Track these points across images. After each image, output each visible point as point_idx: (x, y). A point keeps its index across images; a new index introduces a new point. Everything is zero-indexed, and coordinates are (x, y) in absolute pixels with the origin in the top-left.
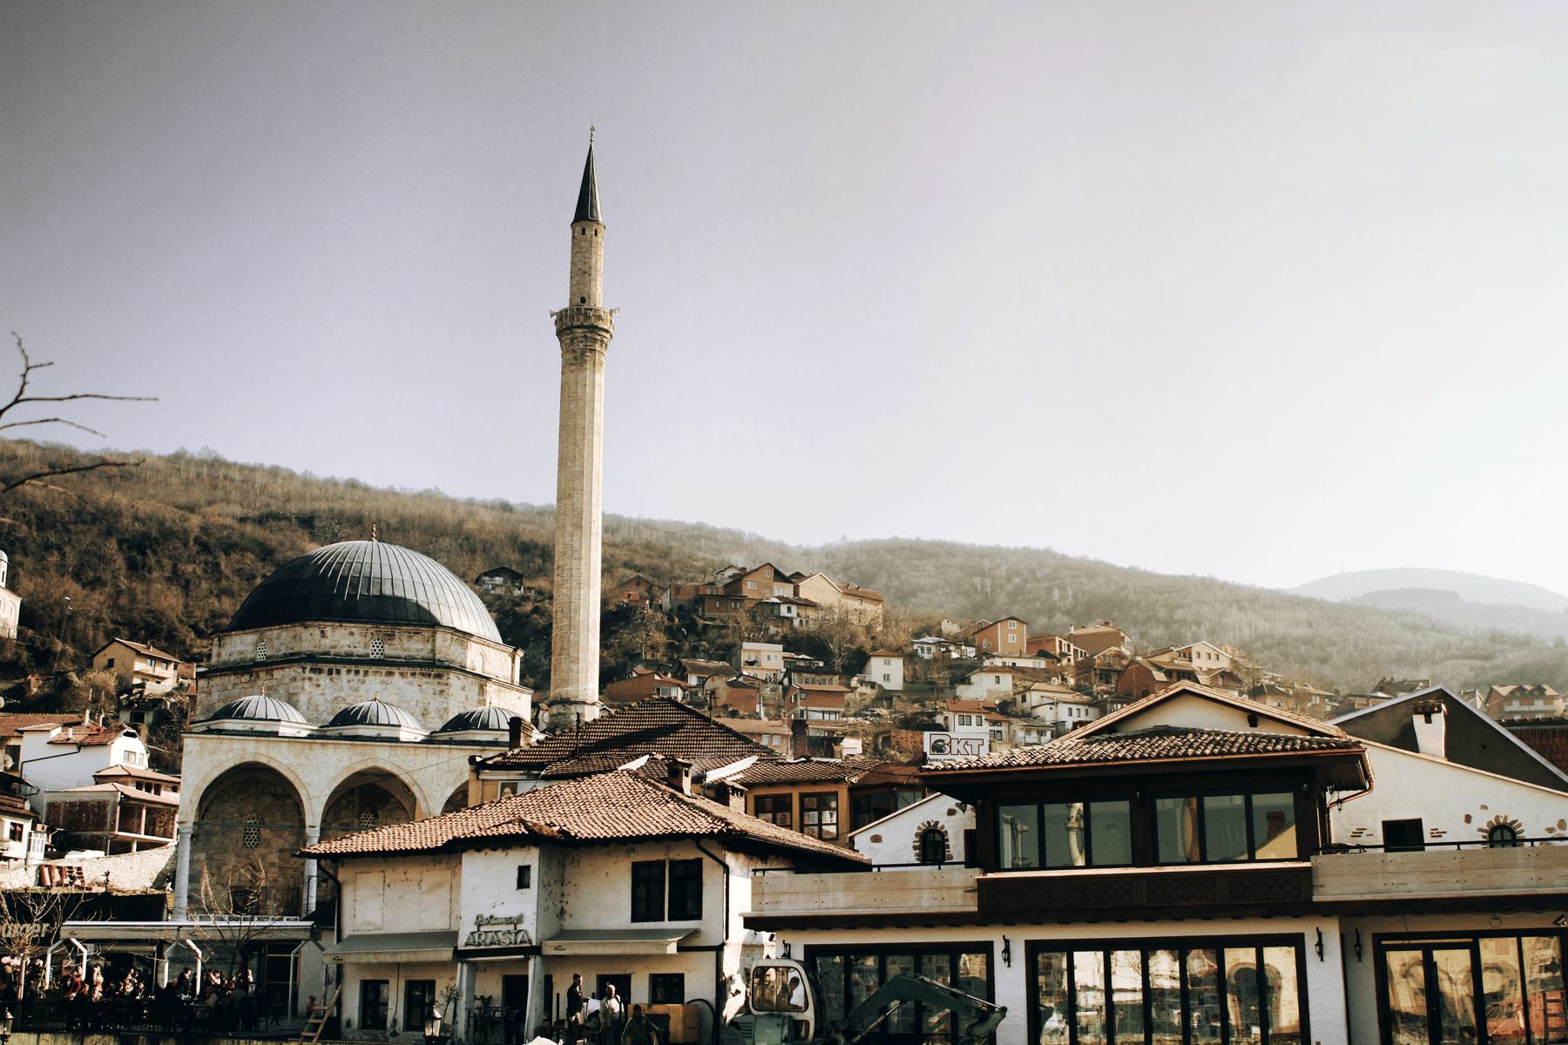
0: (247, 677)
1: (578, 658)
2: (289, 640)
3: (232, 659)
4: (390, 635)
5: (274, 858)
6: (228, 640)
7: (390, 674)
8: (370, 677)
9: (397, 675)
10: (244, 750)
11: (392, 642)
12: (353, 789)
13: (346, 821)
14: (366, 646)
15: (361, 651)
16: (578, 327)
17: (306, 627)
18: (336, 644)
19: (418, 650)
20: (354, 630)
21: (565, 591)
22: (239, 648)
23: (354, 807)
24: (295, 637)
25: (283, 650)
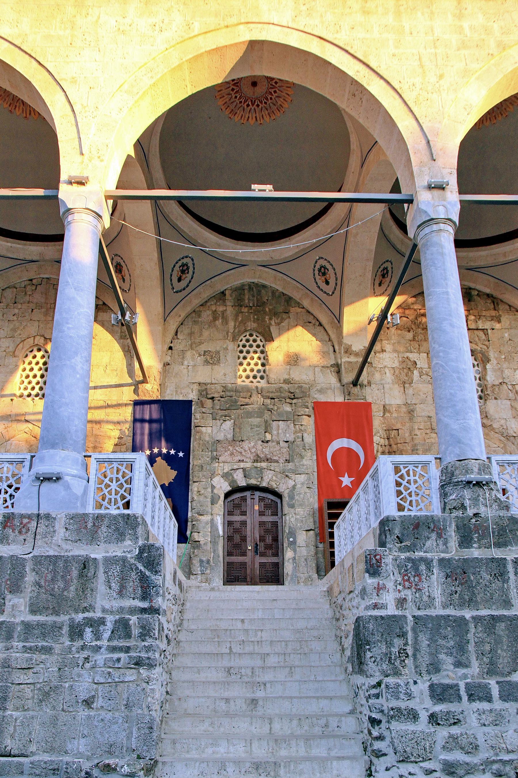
12: (223, 293)
13: (211, 347)
23: (225, 321)
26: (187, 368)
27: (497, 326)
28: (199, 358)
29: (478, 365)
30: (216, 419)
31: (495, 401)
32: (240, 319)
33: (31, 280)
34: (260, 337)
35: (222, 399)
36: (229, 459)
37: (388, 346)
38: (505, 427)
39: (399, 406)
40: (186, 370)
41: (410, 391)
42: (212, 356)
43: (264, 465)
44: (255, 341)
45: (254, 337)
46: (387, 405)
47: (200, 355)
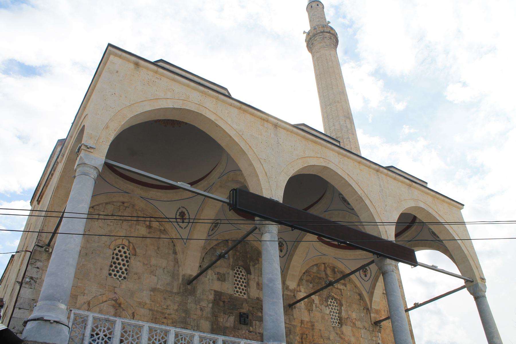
5: (145, 296)
16: (327, 32)
26: (209, 280)
27: (345, 288)
28: (215, 275)
29: (337, 306)
30: (225, 314)
31: (345, 326)
32: (235, 258)
33: (123, 203)
34: (244, 271)
35: (229, 303)
37: (302, 289)
38: (350, 340)
39: (307, 322)
40: (208, 281)
41: (312, 315)
42: (221, 276)
44: (241, 272)
45: (241, 270)
46: (303, 320)
47: (215, 274)
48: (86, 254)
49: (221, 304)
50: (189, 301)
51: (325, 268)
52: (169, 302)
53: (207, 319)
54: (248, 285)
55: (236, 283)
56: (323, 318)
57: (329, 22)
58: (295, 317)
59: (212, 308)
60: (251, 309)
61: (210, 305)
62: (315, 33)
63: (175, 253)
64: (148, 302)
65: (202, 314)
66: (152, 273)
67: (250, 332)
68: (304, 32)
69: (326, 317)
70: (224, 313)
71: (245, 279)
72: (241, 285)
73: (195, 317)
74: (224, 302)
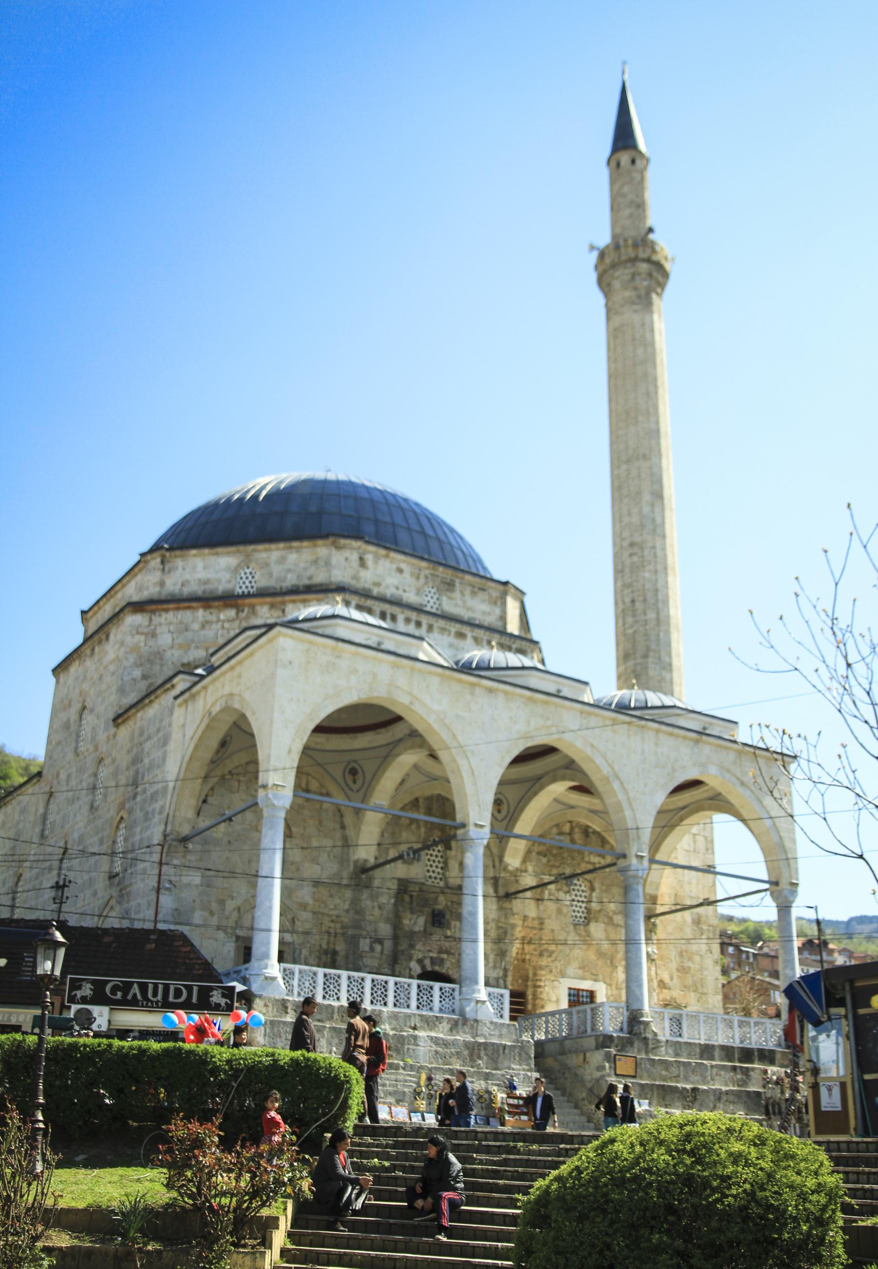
0: (232, 613)
1: (670, 665)
2: (302, 565)
3: (186, 591)
4: (449, 584)
6: (179, 563)
7: (461, 635)
8: (436, 634)
9: (469, 641)
10: (375, 675)
11: (453, 595)
12: (417, 799)
14: (418, 592)
15: (411, 597)
17: (338, 548)
18: (377, 580)
19: (484, 613)
20: (403, 566)
21: (647, 575)
22: (201, 574)
24: (315, 562)
25: (291, 580)
36: (422, 948)
39: (534, 919)
43: (445, 956)
48: (229, 842)
49: (407, 898)
50: (364, 897)
51: (572, 829)
52: (337, 901)
53: (387, 920)
54: (445, 867)
55: (429, 863)
56: (559, 911)
57: (651, 230)
58: (515, 910)
59: (395, 905)
60: (449, 903)
61: (392, 901)
62: (616, 260)
63: (343, 827)
64: (311, 902)
65: (382, 915)
66: (315, 861)
67: (447, 937)
68: (592, 248)
69: (565, 910)
70: (412, 913)
71: (442, 857)
72: (437, 867)
73: (371, 918)
74: (411, 896)
